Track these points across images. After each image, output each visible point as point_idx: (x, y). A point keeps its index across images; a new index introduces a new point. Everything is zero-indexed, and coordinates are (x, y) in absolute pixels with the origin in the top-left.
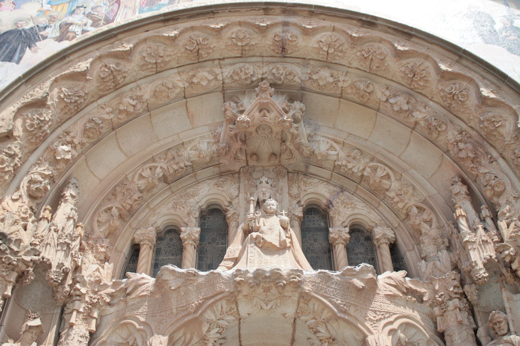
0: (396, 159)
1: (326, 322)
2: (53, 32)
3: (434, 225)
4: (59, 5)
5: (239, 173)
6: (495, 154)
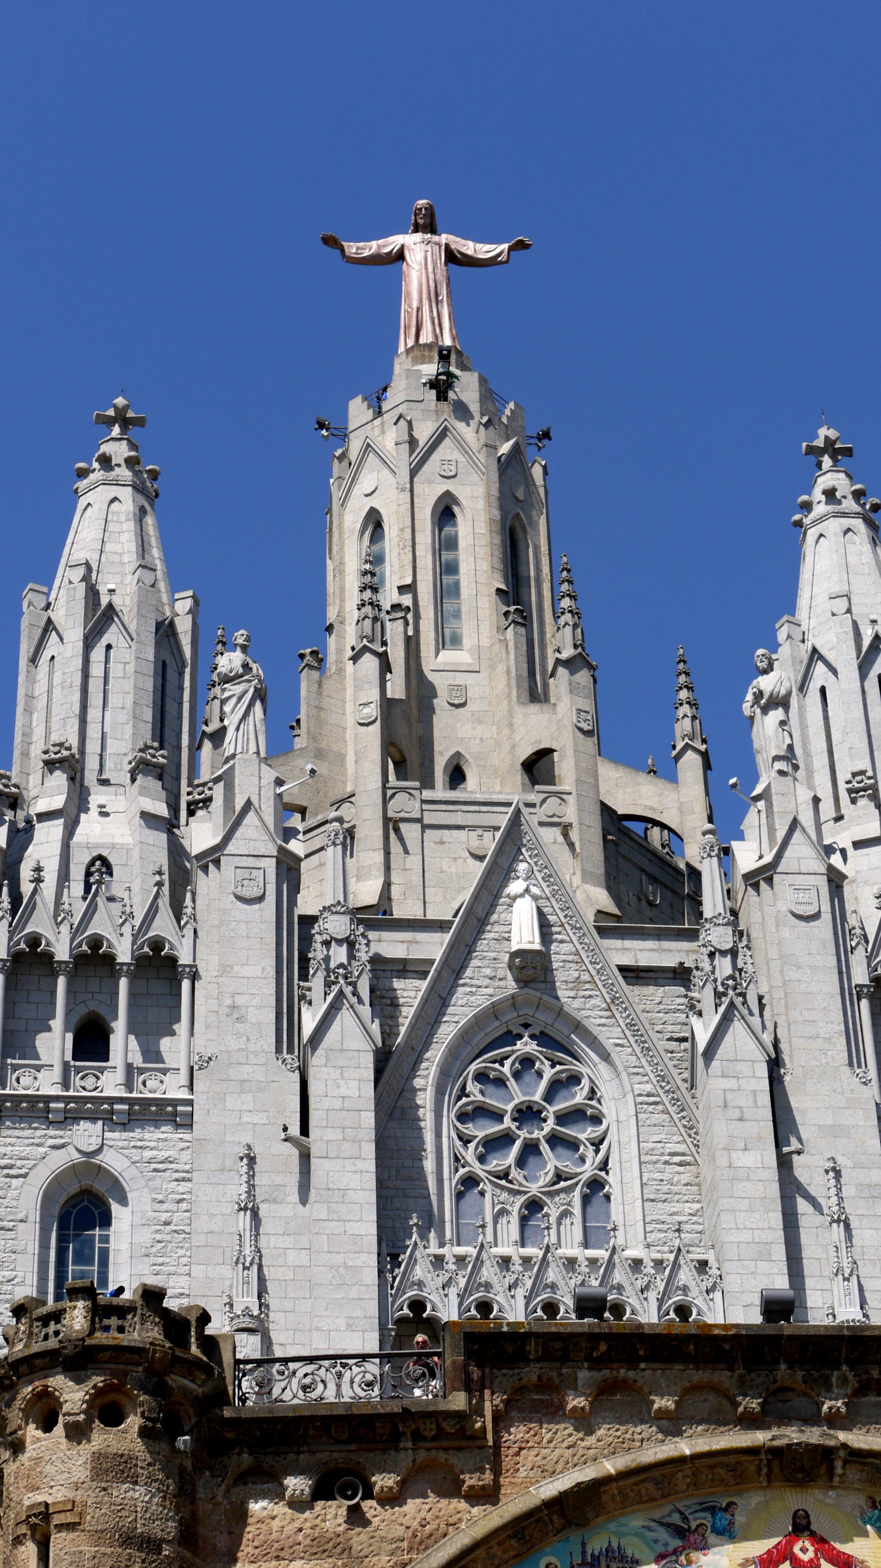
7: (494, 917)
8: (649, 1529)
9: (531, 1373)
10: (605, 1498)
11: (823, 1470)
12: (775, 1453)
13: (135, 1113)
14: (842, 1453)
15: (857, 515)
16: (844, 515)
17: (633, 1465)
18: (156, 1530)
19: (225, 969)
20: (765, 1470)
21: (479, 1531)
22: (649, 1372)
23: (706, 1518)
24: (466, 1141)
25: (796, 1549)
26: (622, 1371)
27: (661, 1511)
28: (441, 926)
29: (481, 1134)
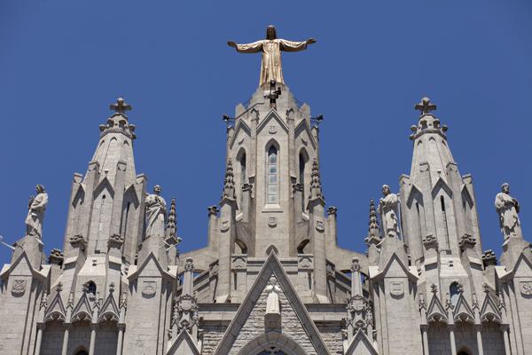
7: (259, 301)
15: (435, 132)
16: (430, 132)
19: (137, 324)
28: (238, 305)
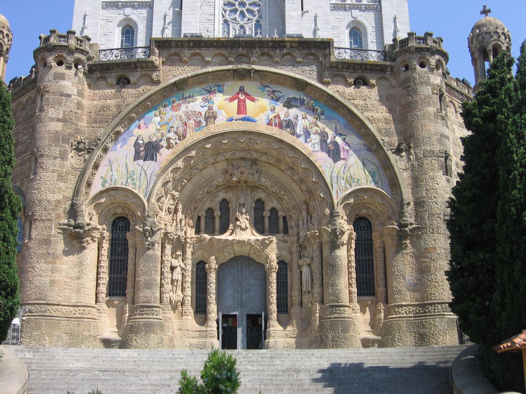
0: (288, 187)
1: (258, 252)
2: (164, 143)
3: (296, 215)
4: (163, 125)
5: (233, 187)
6: (315, 198)
8: (201, 91)
9: (173, 51)
10: (189, 83)
11: (248, 75)
12: (235, 71)
13: (140, 5)
14: (253, 71)
17: (196, 74)
18: (69, 92)
20: (232, 75)
21: (152, 92)
22: (204, 51)
23: (216, 88)
24: (225, 11)
25: (240, 96)
26: (197, 50)
27: (205, 86)
29: (229, 9)
